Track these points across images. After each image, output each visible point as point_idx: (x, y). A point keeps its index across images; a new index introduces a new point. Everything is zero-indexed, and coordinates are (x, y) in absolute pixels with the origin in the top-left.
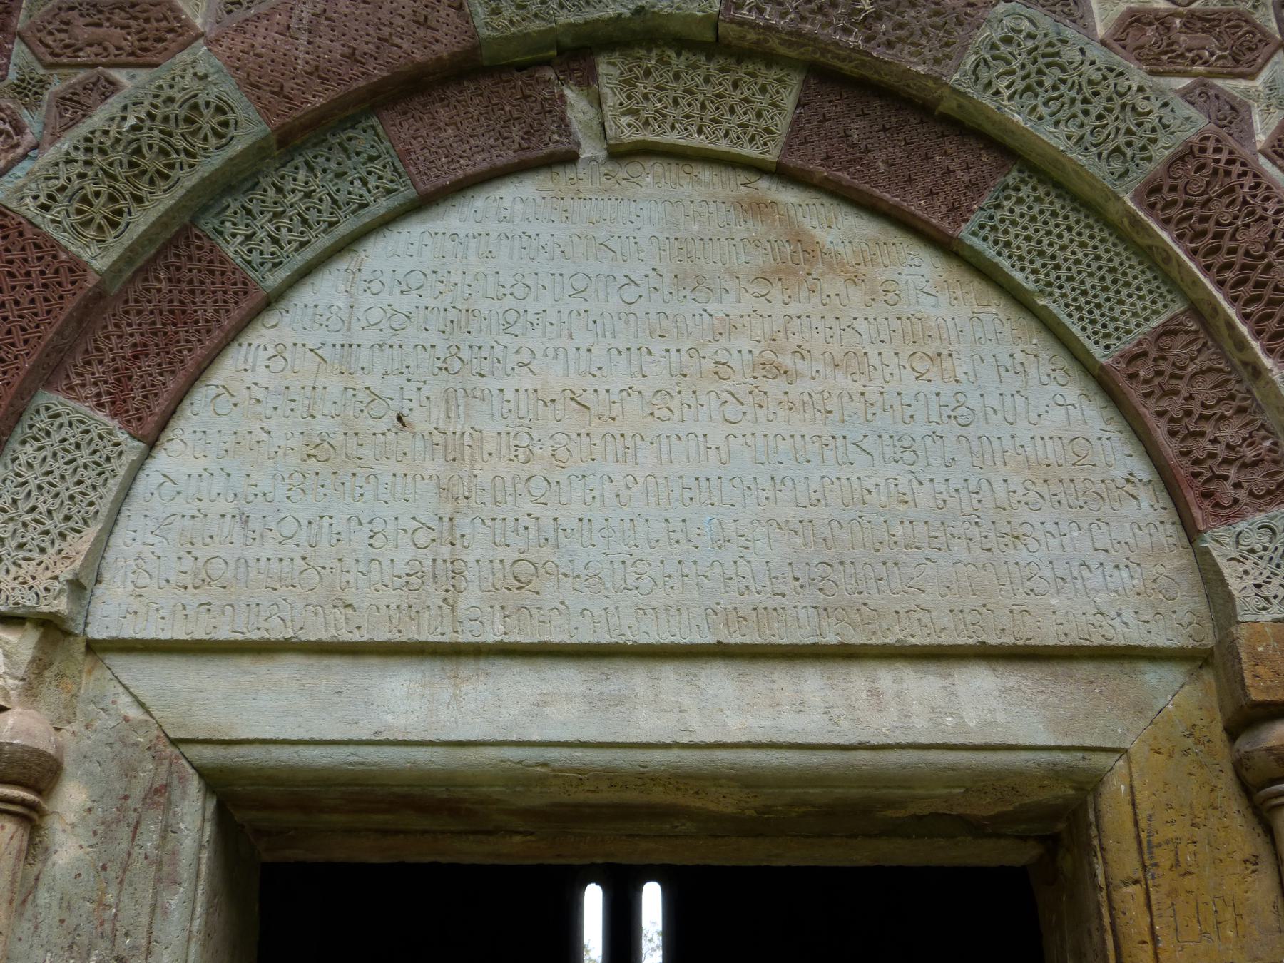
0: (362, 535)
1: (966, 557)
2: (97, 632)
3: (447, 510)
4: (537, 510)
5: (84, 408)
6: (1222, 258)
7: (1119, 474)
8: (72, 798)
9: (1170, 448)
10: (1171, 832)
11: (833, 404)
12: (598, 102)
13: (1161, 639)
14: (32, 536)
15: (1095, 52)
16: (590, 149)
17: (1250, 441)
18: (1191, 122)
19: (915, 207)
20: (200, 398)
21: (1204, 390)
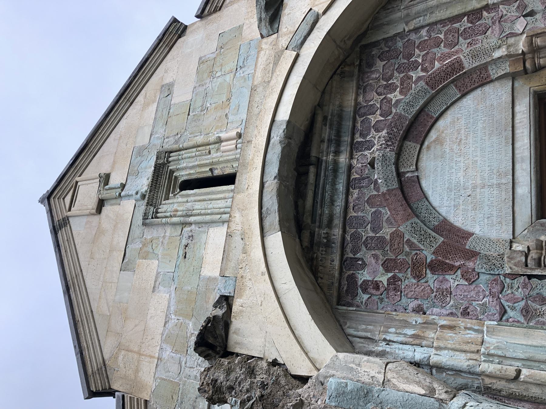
0: (491, 199)
2: (511, 238)
3: (486, 187)
4: (486, 173)
5: (468, 242)
6: (446, 78)
7: (480, 92)
9: (476, 85)
11: (466, 133)
13: (511, 84)
14: (494, 246)
15: (407, 97)
18: (422, 83)
19: (430, 124)
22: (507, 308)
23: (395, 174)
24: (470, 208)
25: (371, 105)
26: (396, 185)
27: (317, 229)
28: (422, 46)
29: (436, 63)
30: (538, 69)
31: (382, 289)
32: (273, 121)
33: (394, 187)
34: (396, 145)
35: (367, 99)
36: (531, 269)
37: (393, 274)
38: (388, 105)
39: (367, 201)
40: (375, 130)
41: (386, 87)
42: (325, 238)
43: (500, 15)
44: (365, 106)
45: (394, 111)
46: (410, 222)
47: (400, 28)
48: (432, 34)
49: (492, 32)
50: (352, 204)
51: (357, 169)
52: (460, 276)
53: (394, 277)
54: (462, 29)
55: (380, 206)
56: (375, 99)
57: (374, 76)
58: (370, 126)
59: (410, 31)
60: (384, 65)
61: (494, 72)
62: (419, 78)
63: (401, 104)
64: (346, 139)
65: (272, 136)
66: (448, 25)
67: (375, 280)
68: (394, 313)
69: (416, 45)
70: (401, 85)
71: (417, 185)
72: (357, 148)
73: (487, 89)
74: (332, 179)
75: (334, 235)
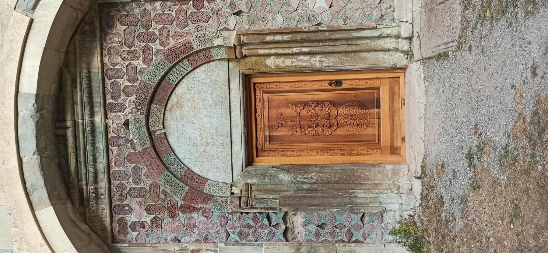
8: (249, 181)
9: (203, 62)
12: (157, 130)
14: (221, 190)
15: (150, 67)
16: (163, 131)
18: (161, 57)
19: (171, 90)
20: (201, 175)
21: (196, 57)
22: (230, 233)
23: (147, 135)
24: (205, 160)
25: (118, 69)
26: (149, 144)
27: (85, 187)
29: (171, 39)
30: (244, 57)
31: (147, 228)
32: (17, 92)
33: (147, 146)
34: (145, 109)
35: (113, 62)
36: (243, 209)
37: (154, 216)
38: (134, 71)
39: (127, 158)
41: (130, 53)
42: (93, 193)
43: (217, 9)
46: (163, 175)
48: (165, 10)
50: (113, 160)
51: (114, 129)
52: (201, 214)
53: (155, 218)
54: (190, 12)
55: (138, 162)
56: (122, 65)
57: (116, 39)
60: (124, 30)
61: (216, 54)
62: (158, 51)
63: (145, 73)
64: (98, 100)
65: (19, 109)
66: (178, 5)
67: (141, 220)
68: (158, 245)
69: (152, 17)
70: (143, 54)
71: (166, 141)
72: (111, 110)
73: (210, 64)
74: (92, 140)
75: (101, 188)
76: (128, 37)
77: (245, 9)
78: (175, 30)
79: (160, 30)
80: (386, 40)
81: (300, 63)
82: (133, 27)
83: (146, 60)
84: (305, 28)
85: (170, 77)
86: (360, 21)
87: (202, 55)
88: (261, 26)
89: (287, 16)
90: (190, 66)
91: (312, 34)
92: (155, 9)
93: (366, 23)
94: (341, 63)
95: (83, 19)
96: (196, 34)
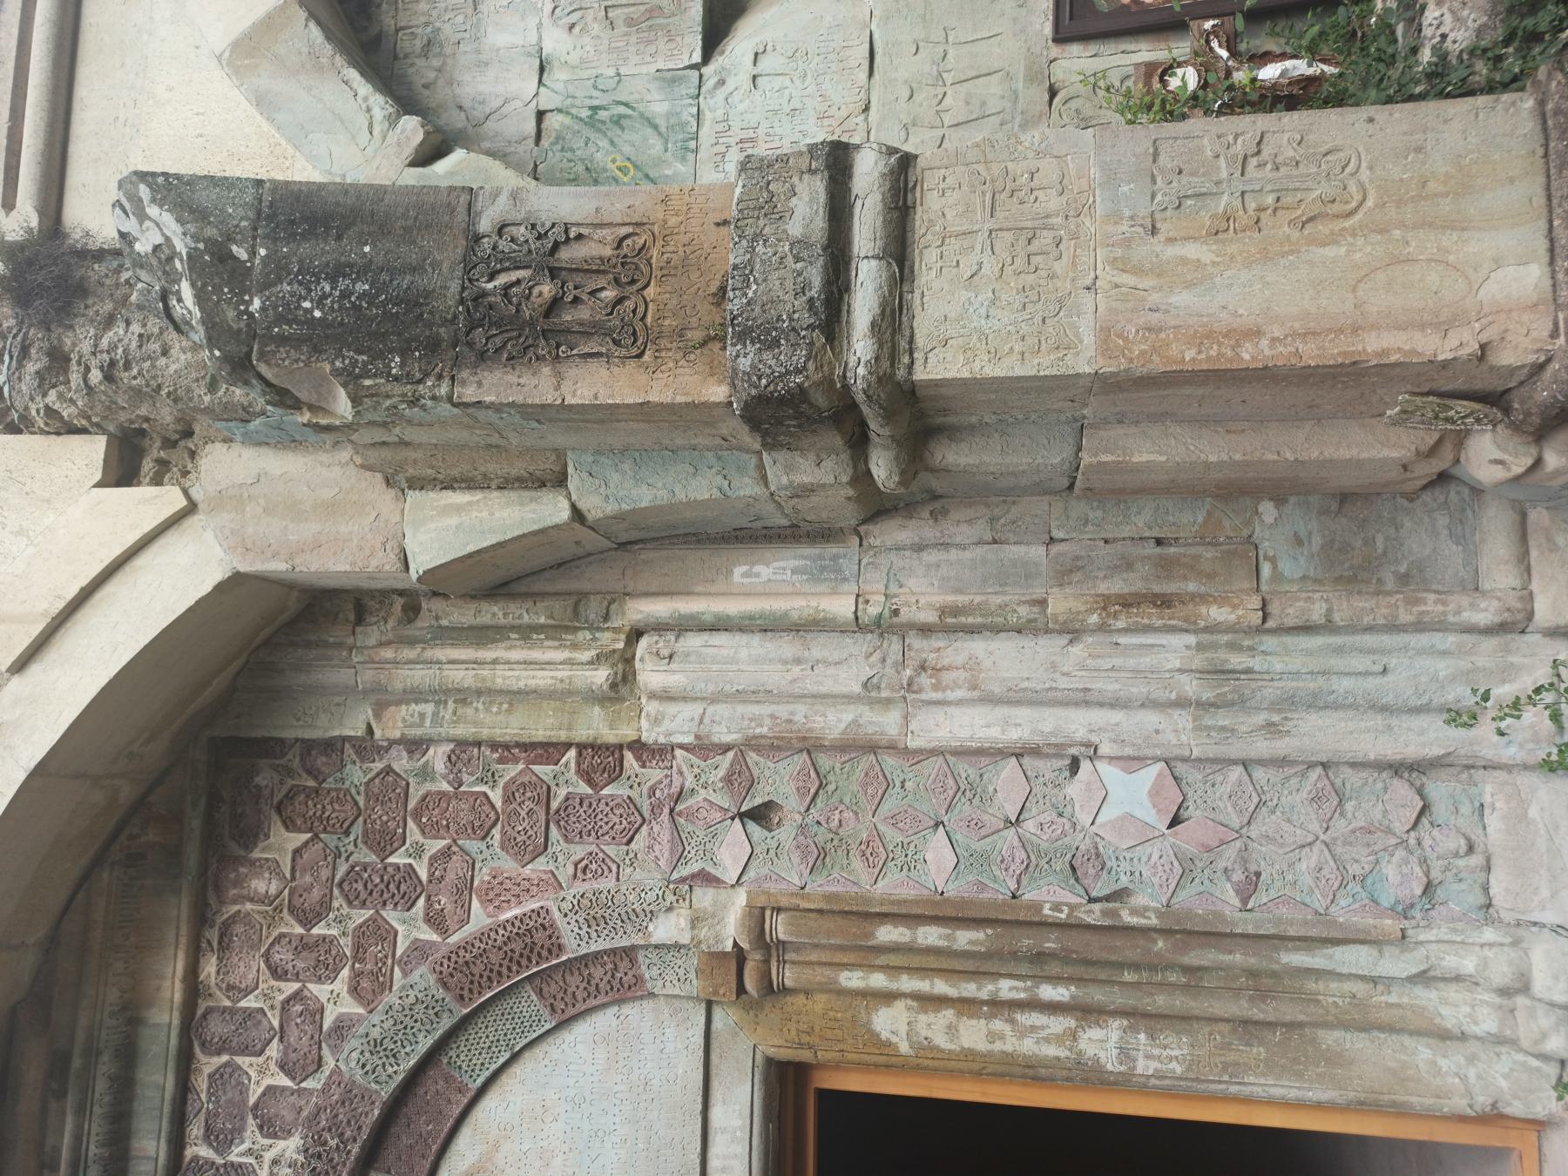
1: (656, 1113)
7: (615, 1022)
9: (602, 999)
10: (794, 1033)
13: (702, 1020)
15: (376, 1018)
17: (603, 965)
18: (423, 976)
19: (457, 1111)
21: (574, 980)
25: (249, 1014)
28: (433, 814)
29: (475, 903)
35: (232, 979)
40: (261, 1128)
43: (675, 790)
44: (225, 1009)
45: (330, 1062)
47: (353, 727)
48: (465, 777)
49: (651, 847)
54: (562, 792)
56: (264, 997)
57: (260, 885)
58: (244, 1101)
59: (393, 743)
60: (297, 852)
62: (420, 950)
63: (355, 1043)
66: (516, 761)
69: (411, 805)
70: (356, 958)
76: (308, 879)
77: (791, 803)
78: (496, 864)
79: (433, 859)
80: (1452, 992)
81: (1028, 1046)
82: (331, 840)
83: (365, 984)
84: (1057, 907)
85: (460, 1054)
86: (1318, 901)
87: (598, 972)
88: (854, 878)
89: (978, 846)
90: (546, 1013)
91: (1088, 936)
92: (426, 774)
93: (1345, 911)
94: (1226, 1066)
95: (140, 804)
96: (580, 887)
